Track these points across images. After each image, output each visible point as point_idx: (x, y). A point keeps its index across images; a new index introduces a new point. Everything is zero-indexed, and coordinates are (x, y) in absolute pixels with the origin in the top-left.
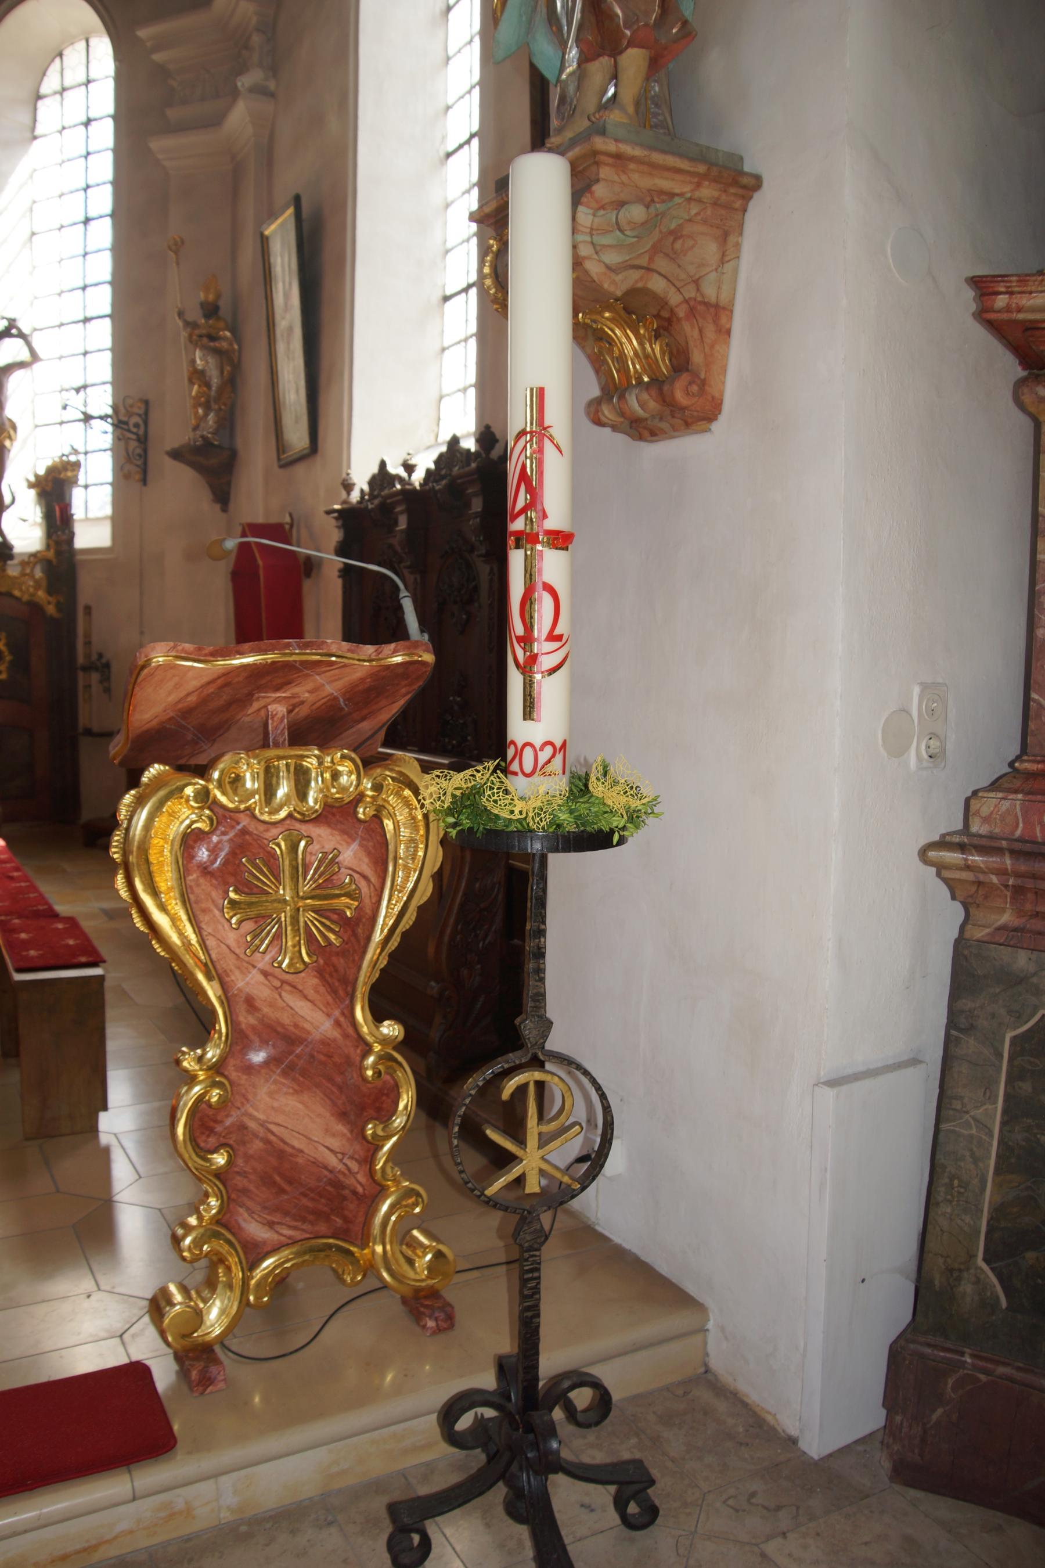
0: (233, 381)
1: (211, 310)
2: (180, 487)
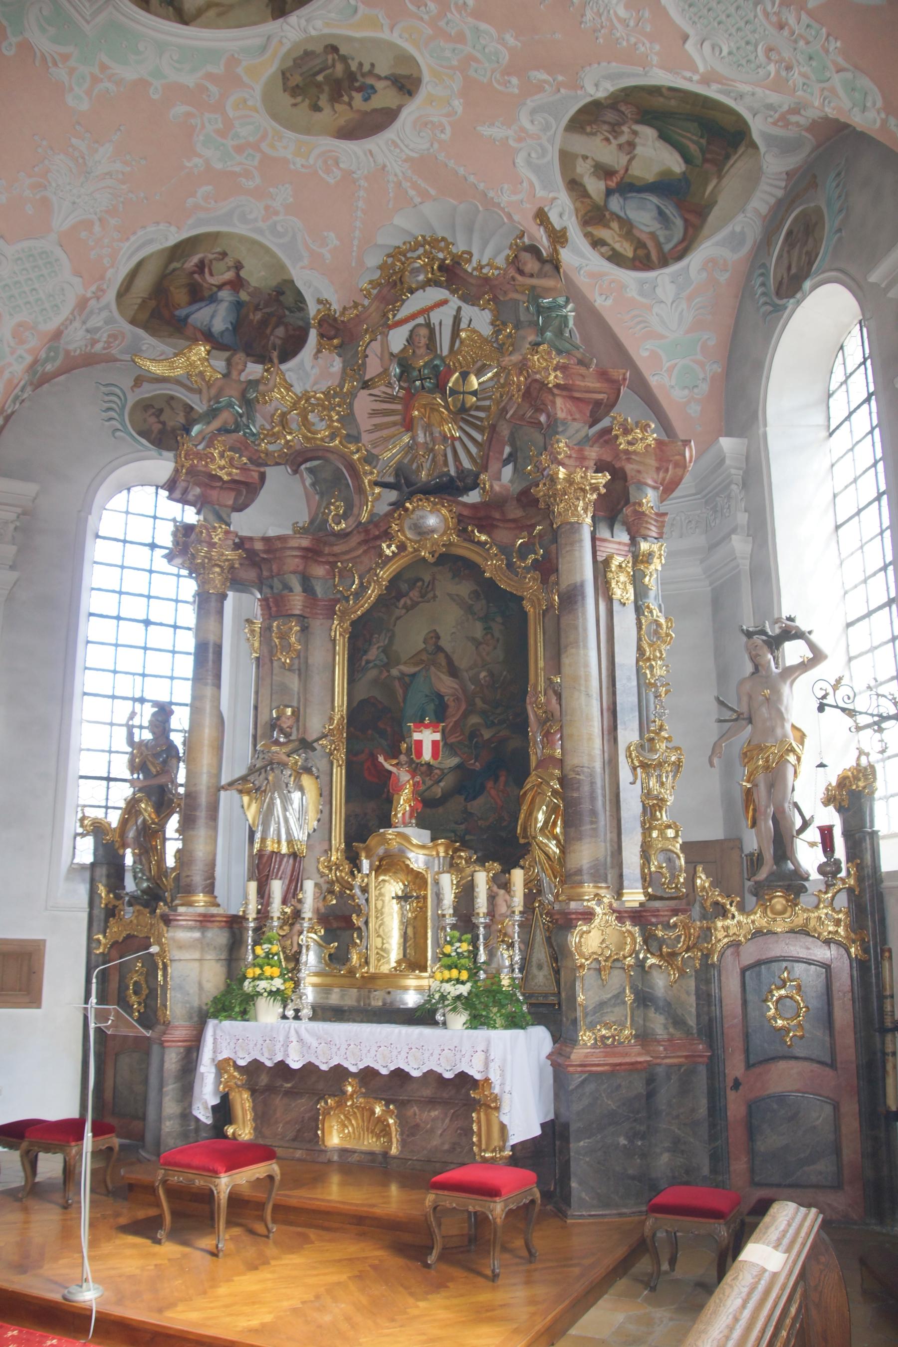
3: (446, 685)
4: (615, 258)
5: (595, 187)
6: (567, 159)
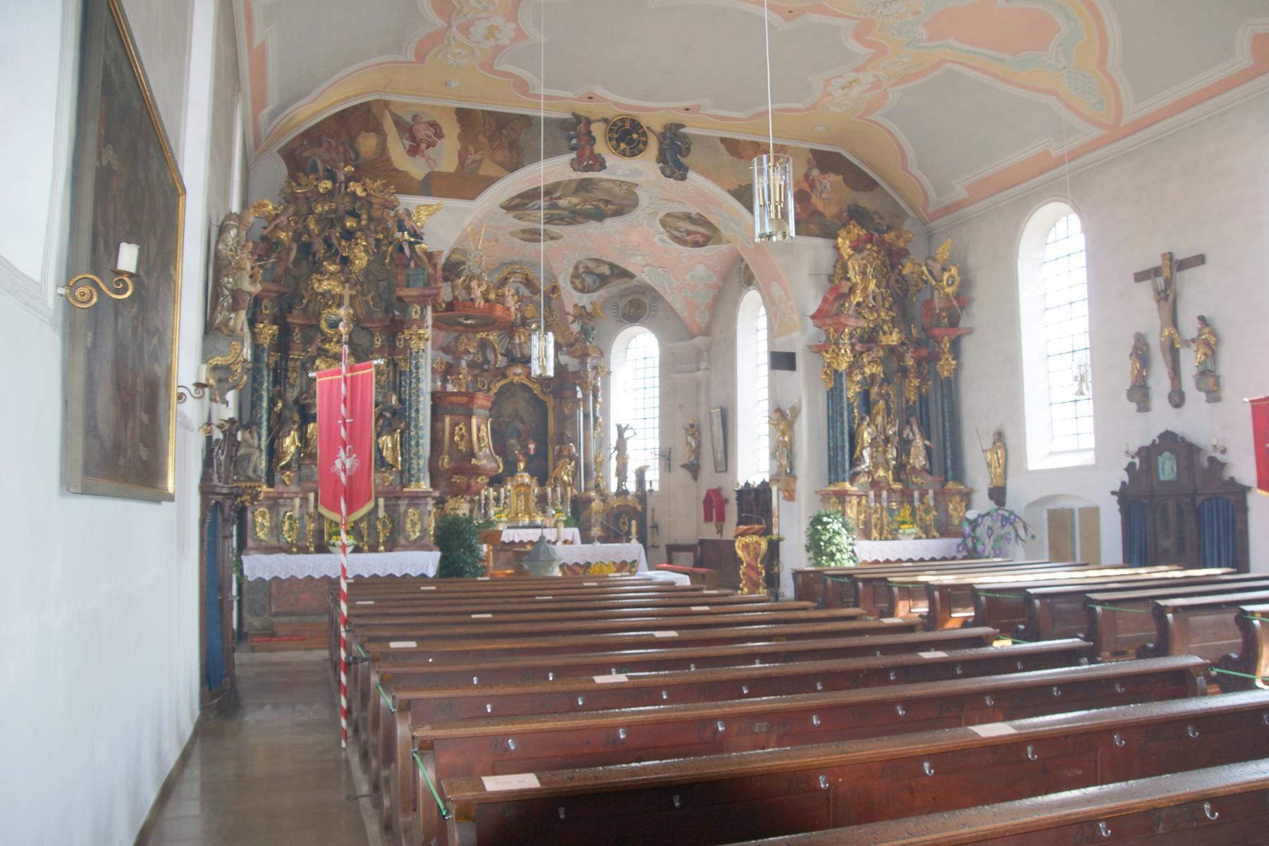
0: (699, 446)
1: (692, 426)
2: (683, 476)
3: (520, 426)
4: (576, 288)
5: (581, 270)
6: (579, 262)
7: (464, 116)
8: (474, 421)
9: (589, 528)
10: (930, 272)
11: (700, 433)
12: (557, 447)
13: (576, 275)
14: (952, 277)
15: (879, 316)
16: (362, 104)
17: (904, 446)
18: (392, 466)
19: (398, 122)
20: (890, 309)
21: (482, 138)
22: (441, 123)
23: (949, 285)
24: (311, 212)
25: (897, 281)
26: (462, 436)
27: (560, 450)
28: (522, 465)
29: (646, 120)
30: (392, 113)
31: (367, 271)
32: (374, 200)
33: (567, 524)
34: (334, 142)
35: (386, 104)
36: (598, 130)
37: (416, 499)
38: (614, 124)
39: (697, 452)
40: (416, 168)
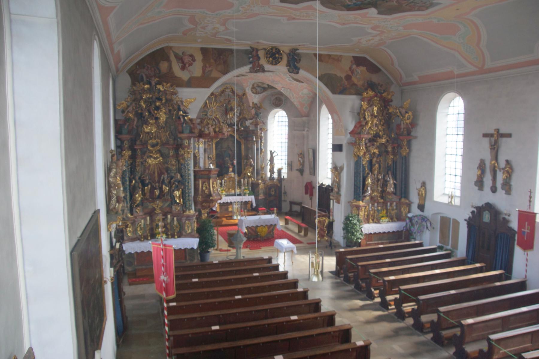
0: (304, 162)
1: (301, 154)
2: (296, 173)
4: (253, 93)
7: (204, 51)
8: (211, 181)
9: (258, 195)
10: (400, 113)
11: (304, 157)
12: (245, 161)
13: (253, 88)
14: (409, 116)
15: (378, 128)
16: (160, 49)
17: (385, 184)
18: (179, 203)
19: (176, 56)
20: (383, 125)
21: (212, 61)
22: (195, 55)
23: (408, 119)
24: (142, 98)
25: (387, 114)
26: (206, 188)
27: (247, 162)
28: (231, 169)
29: (281, 49)
30: (173, 51)
31: (166, 122)
32: (167, 92)
33: (249, 194)
34: (150, 67)
35: (171, 48)
36: (261, 54)
37: (188, 218)
38: (268, 51)
39: (303, 164)
40: (184, 76)
